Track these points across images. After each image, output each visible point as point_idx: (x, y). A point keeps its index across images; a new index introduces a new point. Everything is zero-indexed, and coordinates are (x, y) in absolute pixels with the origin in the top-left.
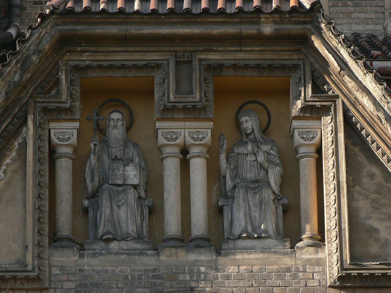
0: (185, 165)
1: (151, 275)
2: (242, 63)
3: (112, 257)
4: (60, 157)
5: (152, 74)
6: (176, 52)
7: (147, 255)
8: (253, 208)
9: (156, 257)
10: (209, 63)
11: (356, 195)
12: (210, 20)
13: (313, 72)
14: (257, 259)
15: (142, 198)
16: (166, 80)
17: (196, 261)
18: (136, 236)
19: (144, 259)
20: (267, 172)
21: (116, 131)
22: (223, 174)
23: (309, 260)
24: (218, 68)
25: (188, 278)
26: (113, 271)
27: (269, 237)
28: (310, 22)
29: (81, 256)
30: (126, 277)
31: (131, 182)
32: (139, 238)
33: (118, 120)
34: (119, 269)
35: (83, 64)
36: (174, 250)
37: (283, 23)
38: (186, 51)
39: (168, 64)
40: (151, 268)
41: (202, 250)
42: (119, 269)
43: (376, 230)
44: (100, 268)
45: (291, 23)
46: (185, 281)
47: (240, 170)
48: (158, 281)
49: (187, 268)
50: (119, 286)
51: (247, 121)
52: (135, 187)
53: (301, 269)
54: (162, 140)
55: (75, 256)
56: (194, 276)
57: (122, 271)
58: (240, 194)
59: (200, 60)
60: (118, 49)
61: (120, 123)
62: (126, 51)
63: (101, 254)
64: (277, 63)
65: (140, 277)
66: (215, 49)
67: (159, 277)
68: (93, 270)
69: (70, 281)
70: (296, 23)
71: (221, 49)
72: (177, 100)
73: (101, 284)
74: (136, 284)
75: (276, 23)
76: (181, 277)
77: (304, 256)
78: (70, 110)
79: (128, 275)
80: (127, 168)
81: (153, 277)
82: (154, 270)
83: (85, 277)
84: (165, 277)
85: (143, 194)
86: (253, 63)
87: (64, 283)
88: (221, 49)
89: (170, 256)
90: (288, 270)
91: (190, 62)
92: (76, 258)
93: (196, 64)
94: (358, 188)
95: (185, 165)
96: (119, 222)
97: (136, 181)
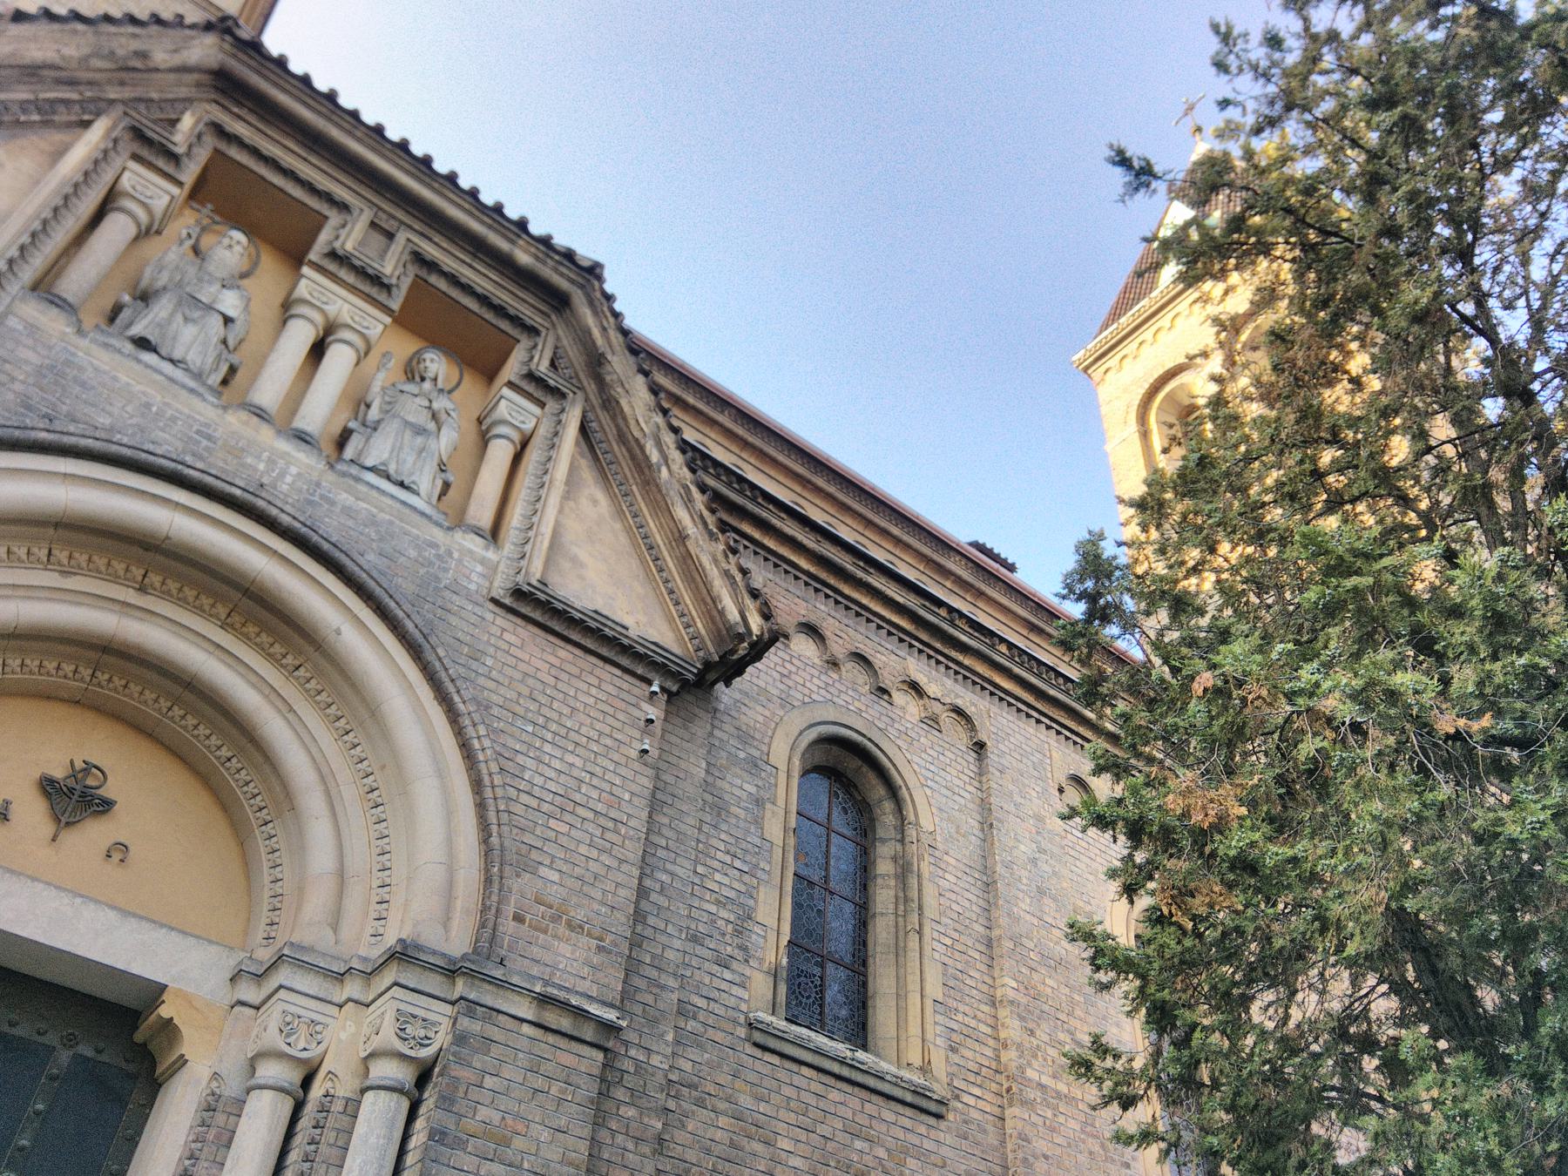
0: (318, 351)
1: (195, 428)
2: (463, 280)
3: (137, 367)
4: (122, 210)
5: (327, 213)
6: (380, 209)
7: (204, 400)
8: (406, 450)
9: (220, 412)
10: (420, 250)
11: (567, 510)
12: (451, 196)
13: (556, 348)
14: (390, 506)
15: (227, 346)
16: (349, 226)
17: (288, 454)
18: (196, 371)
19: (196, 402)
20: (439, 430)
21: (227, 253)
22: (368, 401)
23: (471, 552)
24: (432, 266)
25: (261, 466)
26: (128, 384)
27: (418, 494)
28: (582, 287)
29: (80, 332)
30: (148, 406)
31: (223, 309)
32: (198, 376)
33: (238, 242)
34: (139, 387)
35: (228, 129)
36: (255, 419)
37: (544, 263)
38: (394, 217)
39: (360, 215)
40: (202, 419)
41: (308, 447)
42: (139, 387)
43: (583, 565)
44: (107, 368)
45: (556, 270)
46: (255, 469)
47: (398, 407)
48: (205, 443)
49: (266, 454)
50: (129, 409)
51: (432, 360)
52: (228, 320)
53: (456, 555)
54: (303, 289)
55: (68, 325)
56: (273, 471)
57: (144, 393)
58: (390, 429)
59: (408, 240)
60: (296, 149)
61: (238, 249)
62: (305, 159)
63: (119, 351)
64: (512, 312)
65: (173, 419)
66: (436, 240)
67: (209, 438)
68: (92, 364)
69: (35, 350)
70: (562, 275)
71: (445, 245)
72: (356, 254)
73: (93, 388)
74: (161, 424)
75: (537, 258)
76: (249, 460)
77: (465, 543)
78: (174, 158)
79: (152, 405)
80: (225, 291)
81: (198, 432)
82: (207, 425)
83: (68, 363)
84: (220, 443)
85: (231, 343)
86: (479, 290)
87: (20, 348)
88: (445, 245)
89: (246, 423)
90: (434, 545)
91: (390, 236)
92: (68, 330)
93: (402, 236)
94: (571, 504)
95: (318, 351)
96: (174, 338)
97: (231, 313)
